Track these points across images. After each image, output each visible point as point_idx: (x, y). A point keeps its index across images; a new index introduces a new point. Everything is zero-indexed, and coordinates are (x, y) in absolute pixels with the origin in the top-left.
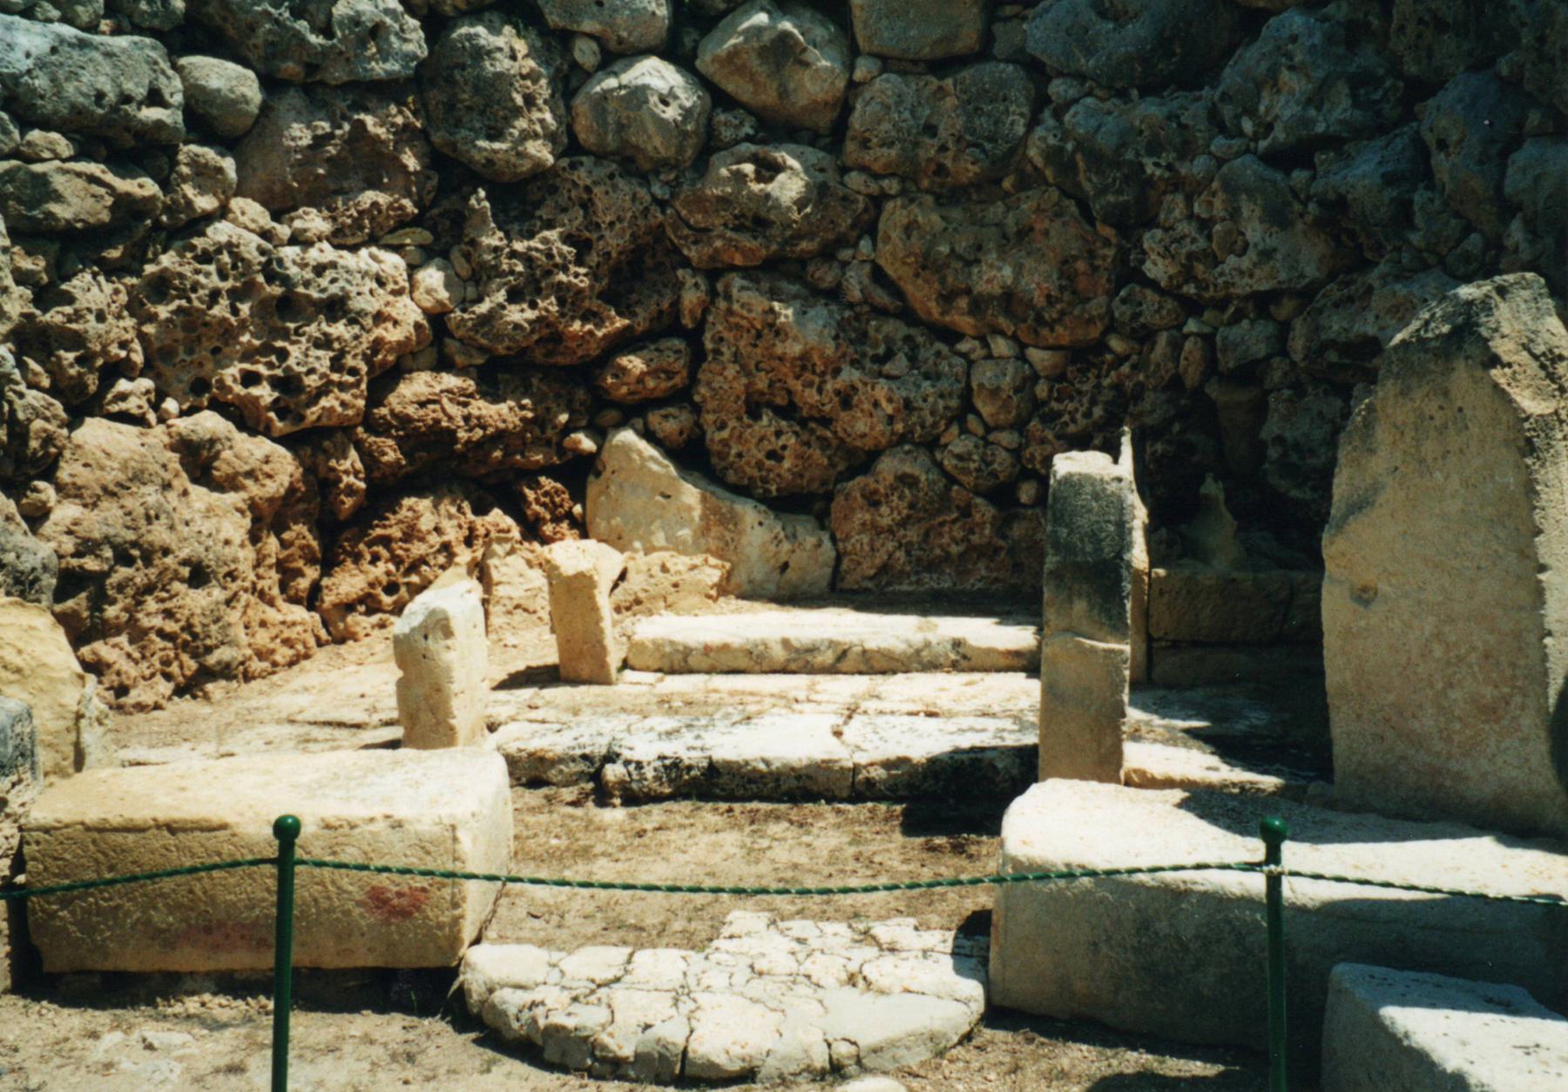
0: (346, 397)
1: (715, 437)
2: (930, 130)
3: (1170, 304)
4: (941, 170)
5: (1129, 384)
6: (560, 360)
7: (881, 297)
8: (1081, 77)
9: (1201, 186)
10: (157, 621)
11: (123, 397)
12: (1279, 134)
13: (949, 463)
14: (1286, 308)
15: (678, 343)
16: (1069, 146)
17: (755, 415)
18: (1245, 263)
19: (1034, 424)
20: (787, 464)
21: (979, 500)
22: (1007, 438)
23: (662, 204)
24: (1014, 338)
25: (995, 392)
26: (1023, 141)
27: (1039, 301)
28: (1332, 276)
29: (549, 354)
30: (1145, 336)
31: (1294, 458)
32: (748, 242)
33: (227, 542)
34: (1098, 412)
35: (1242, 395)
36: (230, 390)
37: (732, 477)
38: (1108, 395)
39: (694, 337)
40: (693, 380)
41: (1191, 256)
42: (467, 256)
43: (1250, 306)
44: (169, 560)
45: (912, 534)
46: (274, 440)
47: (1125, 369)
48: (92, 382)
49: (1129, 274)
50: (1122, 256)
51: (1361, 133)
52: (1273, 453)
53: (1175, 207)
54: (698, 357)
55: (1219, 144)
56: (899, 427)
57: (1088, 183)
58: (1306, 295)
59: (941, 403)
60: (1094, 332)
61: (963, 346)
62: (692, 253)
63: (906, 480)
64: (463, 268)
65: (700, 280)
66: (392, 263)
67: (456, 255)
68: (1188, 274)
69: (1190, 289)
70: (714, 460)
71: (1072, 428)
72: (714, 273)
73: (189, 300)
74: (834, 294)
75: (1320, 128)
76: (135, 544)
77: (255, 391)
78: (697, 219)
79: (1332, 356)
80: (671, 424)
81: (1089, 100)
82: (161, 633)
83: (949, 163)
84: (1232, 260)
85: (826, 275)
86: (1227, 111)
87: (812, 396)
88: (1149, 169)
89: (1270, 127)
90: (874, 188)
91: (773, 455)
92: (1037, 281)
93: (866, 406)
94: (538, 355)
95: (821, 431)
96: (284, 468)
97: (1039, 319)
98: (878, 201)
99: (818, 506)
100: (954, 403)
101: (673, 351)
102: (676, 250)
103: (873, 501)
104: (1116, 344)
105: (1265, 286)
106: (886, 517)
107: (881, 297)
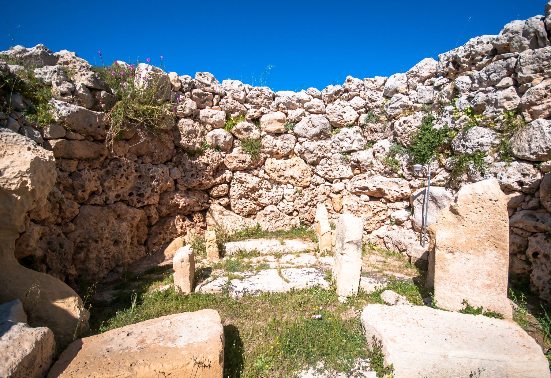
0: (155, 198)
1: (232, 204)
2: (276, 146)
3: (323, 179)
4: (277, 154)
5: (315, 194)
6: (203, 189)
7: (266, 176)
8: (305, 137)
9: (329, 158)
10: (105, 256)
11: (96, 200)
12: (344, 149)
13: (281, 208)
14: (344, 181)
15: (226, 185)
16: (303, 150)
17: (241, 199)
18: (338, 172)
19: (296, 201)
20: (248, 209)
21: (286, 215)
22: (292, 204)
23: (224, 158)
24: (293, 185)
25: (289, 195)
26: (293, 149)
27: (298, 178)
28: (355, 175)
29: (199, 187)
30: (318, 185)
31: (349, 208)
32: (241, 165)
33: (124, 234)
34: (309, 199)
35: (339, 196)
36: (126, 197)
37: (236, 212)
38: (311, 196)
39: (229, 184)
40: (229, 192)
41: (327, 171)
42: (182, 167)
43: (339, 180)
44: (109, 241)
45: (273, 221)
46: (138, 208)
47: (314, 191)
48: (87, 197)
49: (314, 173)
50: (313, 170)
51: (360, 150)
52: (345, 207)
53: (323, 161)
54: (230, 187)
55: (333, 151)
56: (271, 202)
57: (307, 156)
58: (350, 179)
59: (279, 197)
60: (308, 184)
61: (283, 186)
62: (229, 167)
63: (272, 211)
64: (182, 170)
65: (231, 172)
66: (166, 168)
67: (180, 167)
68: (326, 174)
69: (327, 176)
70: (232, 208)
71: (304, 202)
72: (234, 171)
73: (115, 176)
74: (257, 176)
75: (353, 149)
76: (98, 238)
77: (131, 198)
78: (231, 161)
79: (357, 190)
80: (225, 201)
81: (307, 142)
82: (105, 258)
83: (279, 151)
84: (335, 172)
85: (256, 172)
86: (334, 145)
87: (253, 195)
88: (319, 155)
89: (342, 148)
90: (265, 156)
91: (245, 207)
92: (297, 175)
93: (264, 197)
94: (197, 188)
95: (254, 202)
96: (140, 214)
97: (298, 181)
98: (265, 158)
99: (253, 216)
100: (282, 197)
101: (225, 186)
102: (226, 167)
103: (266, 215)
104: (311, 185)
105: (342, 177)
106: (268, 218)
107: (266, 176)
